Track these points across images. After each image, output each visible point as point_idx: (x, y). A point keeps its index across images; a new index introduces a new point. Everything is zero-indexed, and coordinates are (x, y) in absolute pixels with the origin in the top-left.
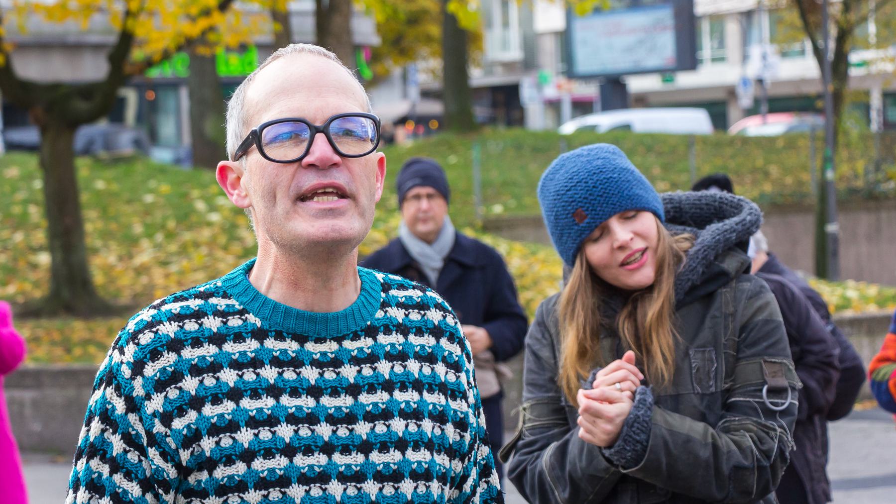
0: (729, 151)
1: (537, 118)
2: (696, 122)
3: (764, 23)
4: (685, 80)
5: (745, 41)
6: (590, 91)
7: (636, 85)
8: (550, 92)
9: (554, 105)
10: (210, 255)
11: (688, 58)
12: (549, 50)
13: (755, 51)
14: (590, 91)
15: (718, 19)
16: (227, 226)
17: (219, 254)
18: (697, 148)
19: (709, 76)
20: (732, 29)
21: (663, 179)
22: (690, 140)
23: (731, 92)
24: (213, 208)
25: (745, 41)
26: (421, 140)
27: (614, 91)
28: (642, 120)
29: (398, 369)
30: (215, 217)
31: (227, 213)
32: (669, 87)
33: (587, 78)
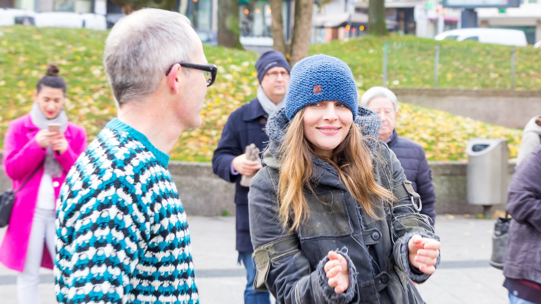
0: (535, 57)
1: (423, 29)
2: (518, 38)
4: (512, 12)
6: (456, 15)
8: (432, 14)
9: (434, 22)
10: (224, 99)
14: (456, 15)
16: (235, 81)
17: (230, 99)
18: (516, 54)
19: (526, 11)
21: (495, 72)
22: (512, 50)
24: (228, 72)
26: (354, 38)
28: (485, 35)
30: (228, 77)
31: (235, 74)
32: (502, 15)
33: (455, 7)
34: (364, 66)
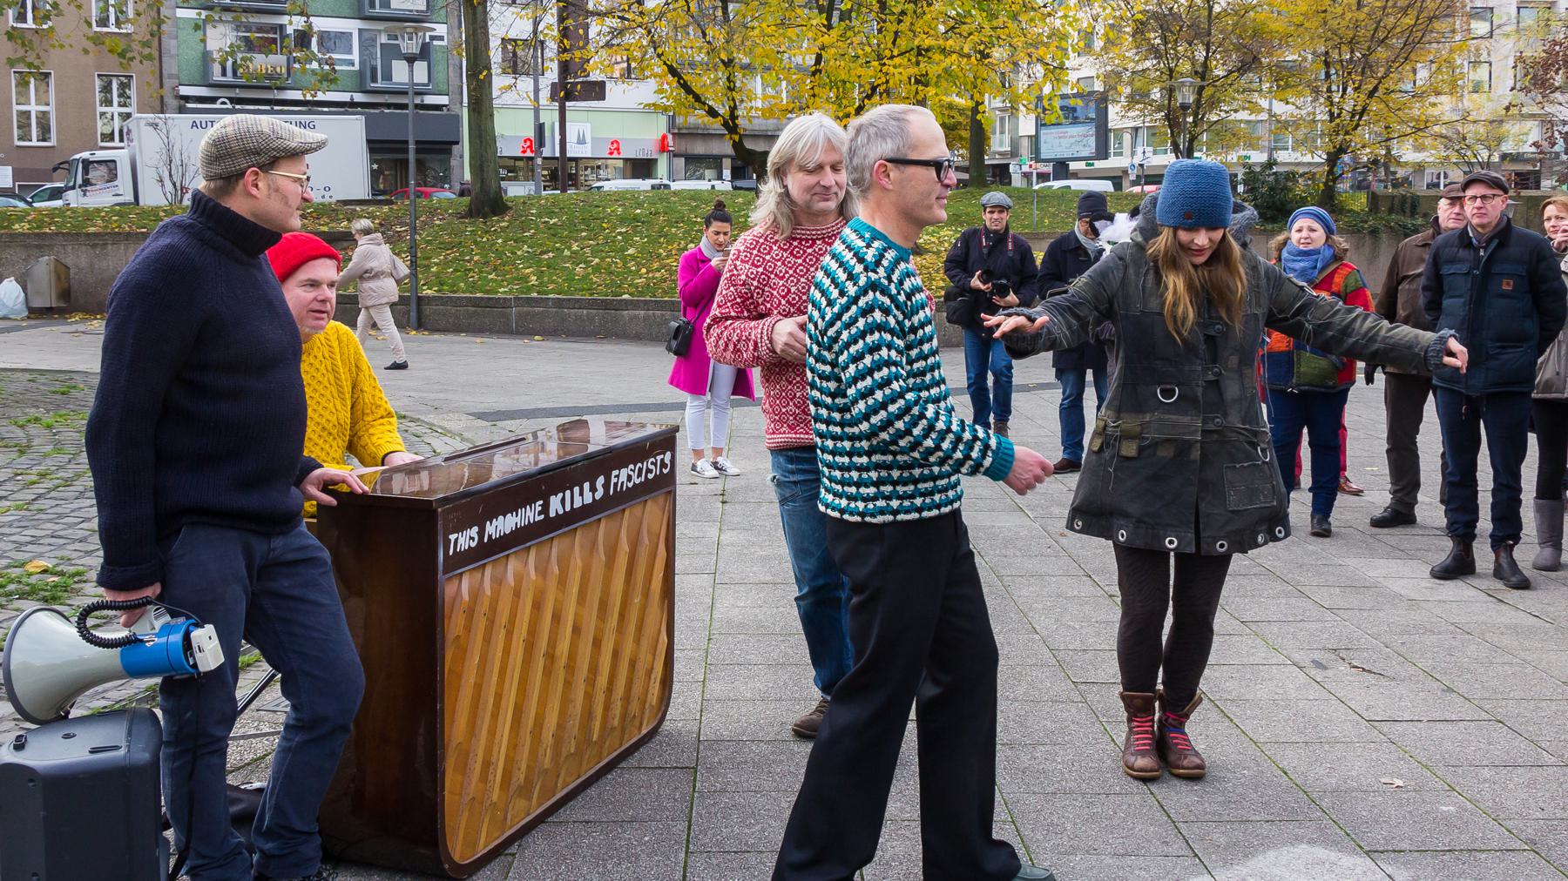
1: (1017, 181)
3: (1143, 135)
4: (1099, 164)
5: (1134, 145)
6: (1049, 168)
7: (1073, 166)
8: (1026, 169)
9: (1027, 176)
11: (1102, 152)
12: (1025, 146)
13: (1139, 150)
14: (1049, 168)
15: (1119, 132)
19: (1113, 162)
20: (1127, 137)
23: (1125, 172)
25: (1134, 145)
27: (1062, 168)
28: (1076, 185)
34: (967, 215)
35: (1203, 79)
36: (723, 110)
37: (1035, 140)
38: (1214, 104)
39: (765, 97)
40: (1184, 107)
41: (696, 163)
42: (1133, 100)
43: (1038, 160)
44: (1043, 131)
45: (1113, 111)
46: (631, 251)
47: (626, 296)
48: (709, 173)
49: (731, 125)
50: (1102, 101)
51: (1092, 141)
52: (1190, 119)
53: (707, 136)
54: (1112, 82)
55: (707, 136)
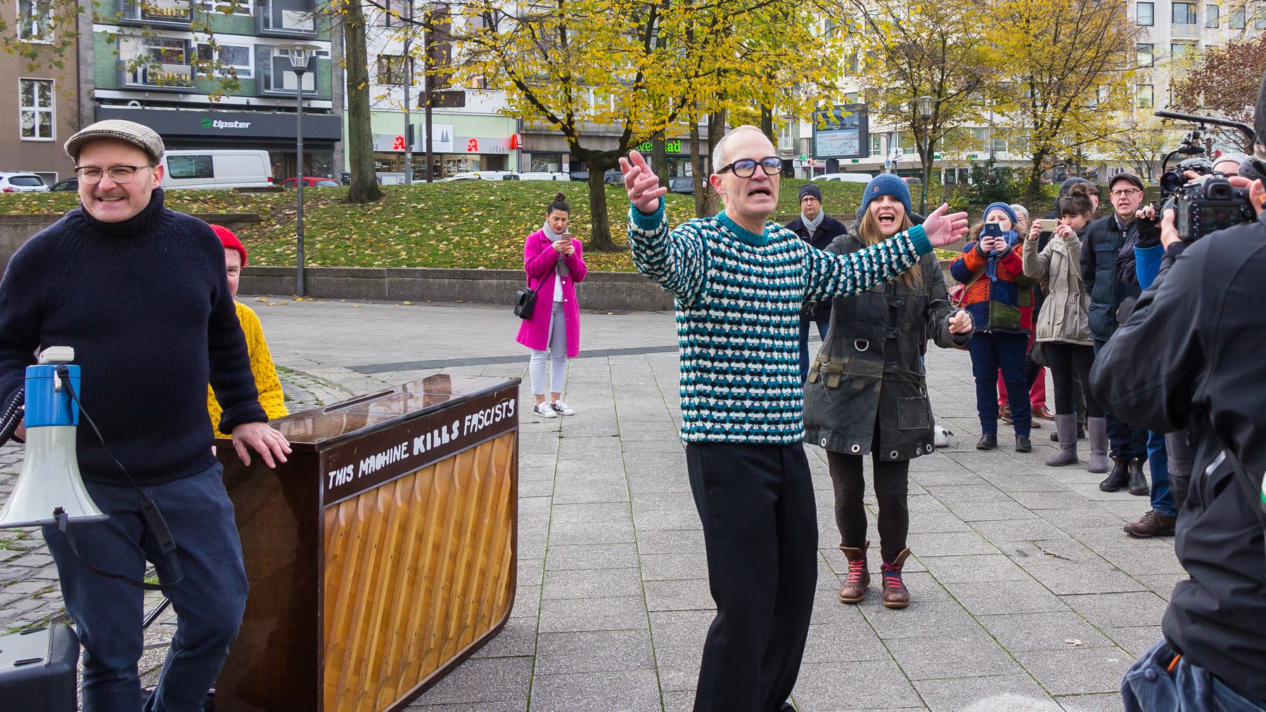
1: (799, 174)
3: (895, 138)
4: (862, 161)
5: (889, 146)
6: (823, 164)
7: (842, 162)
8: (805, 164)
9: (806, 169)
11: (864, 151)
12: (805, 146)
13: (893, 150)
14: (823, 164)
19: (872, 160)
20: (883, 140)
27: (833, 164)
28: (845, 177)
29: (746, 279)
35: (939, 96)
36: (561, 116)
37: (812, 141)
38: (948, 115)
39: (596, 108)
40: (925, 118)
41: (540, 158)
42: (886, 112)
43: (815, 157)
44: (818, 135)
45: (872, 120)
46: (486, 231)
47: (481, 268)
48: (551, 166)
49: (568, 130)
50: (864, 112)
51: (856, 143)
52: (931, 127)
53: (549, 136)
54: (870, 98)
55: (549, 136)
